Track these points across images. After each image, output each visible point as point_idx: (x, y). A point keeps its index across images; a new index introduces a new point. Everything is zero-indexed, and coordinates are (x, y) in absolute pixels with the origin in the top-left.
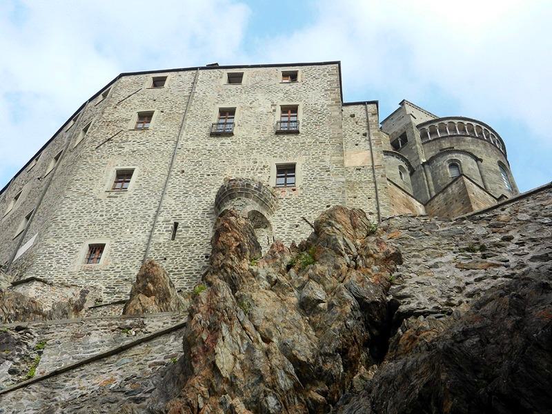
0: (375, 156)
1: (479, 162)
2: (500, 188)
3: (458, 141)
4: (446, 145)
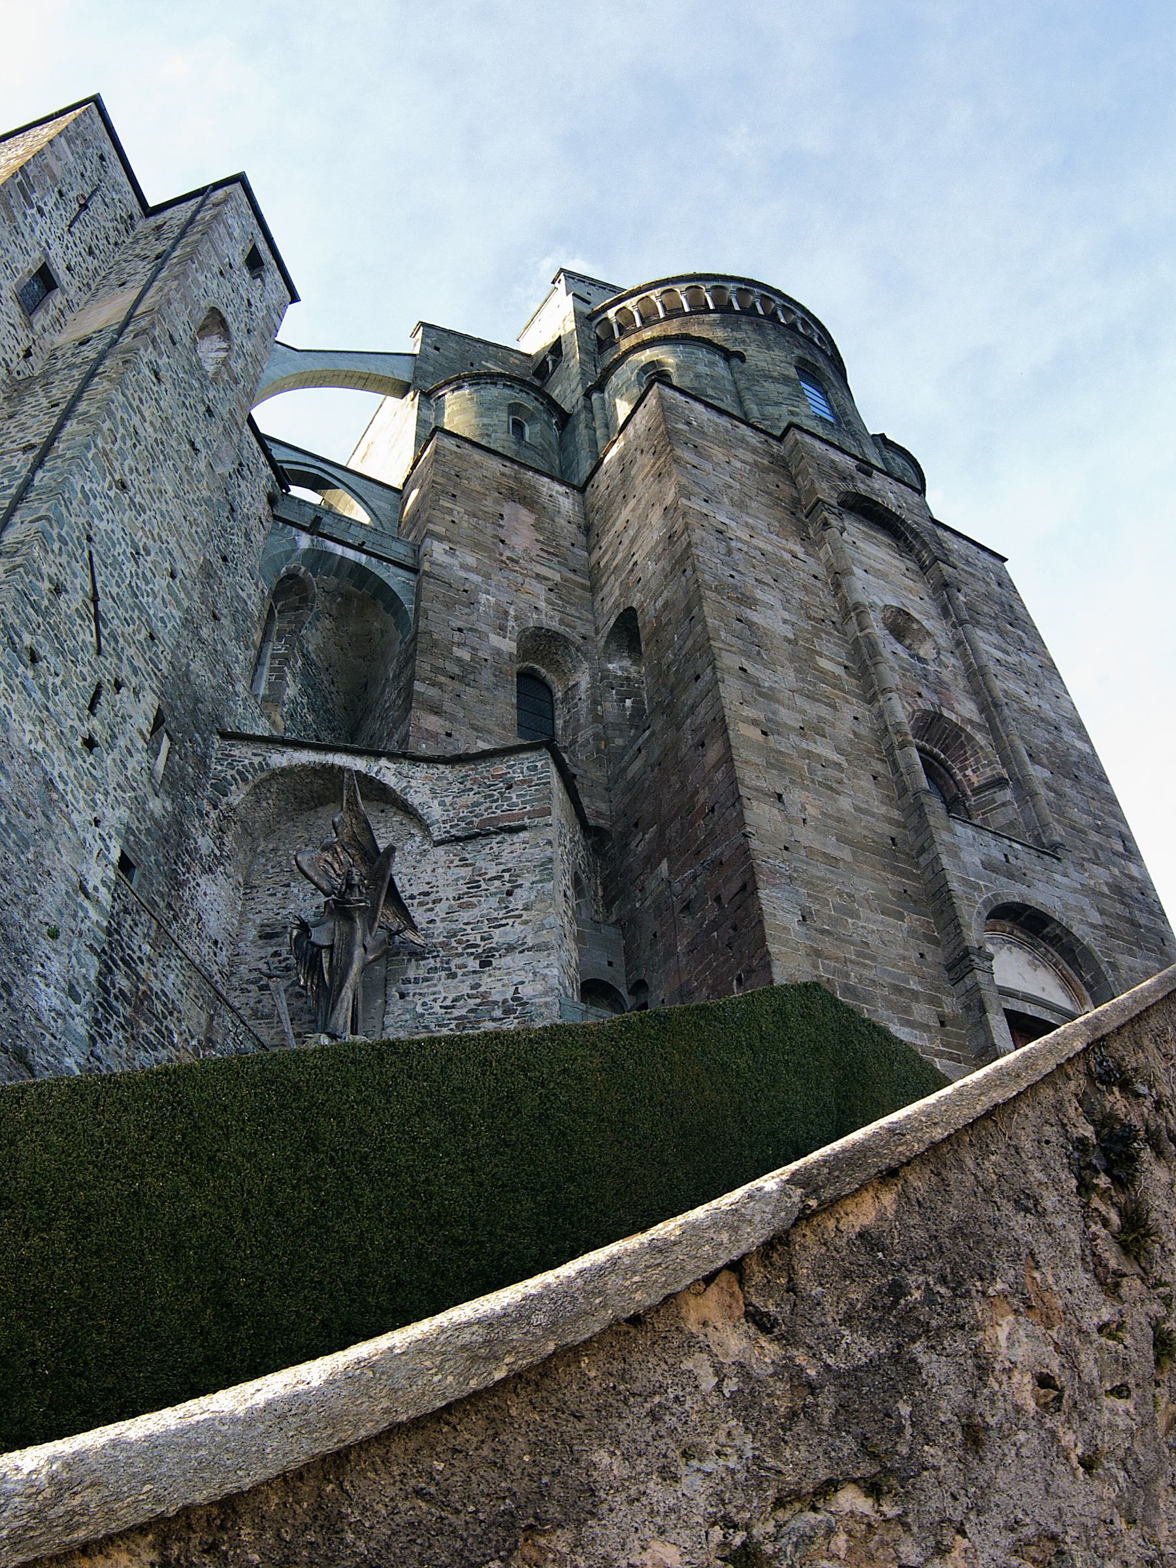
1: (735, 362)
2: (792, 413)
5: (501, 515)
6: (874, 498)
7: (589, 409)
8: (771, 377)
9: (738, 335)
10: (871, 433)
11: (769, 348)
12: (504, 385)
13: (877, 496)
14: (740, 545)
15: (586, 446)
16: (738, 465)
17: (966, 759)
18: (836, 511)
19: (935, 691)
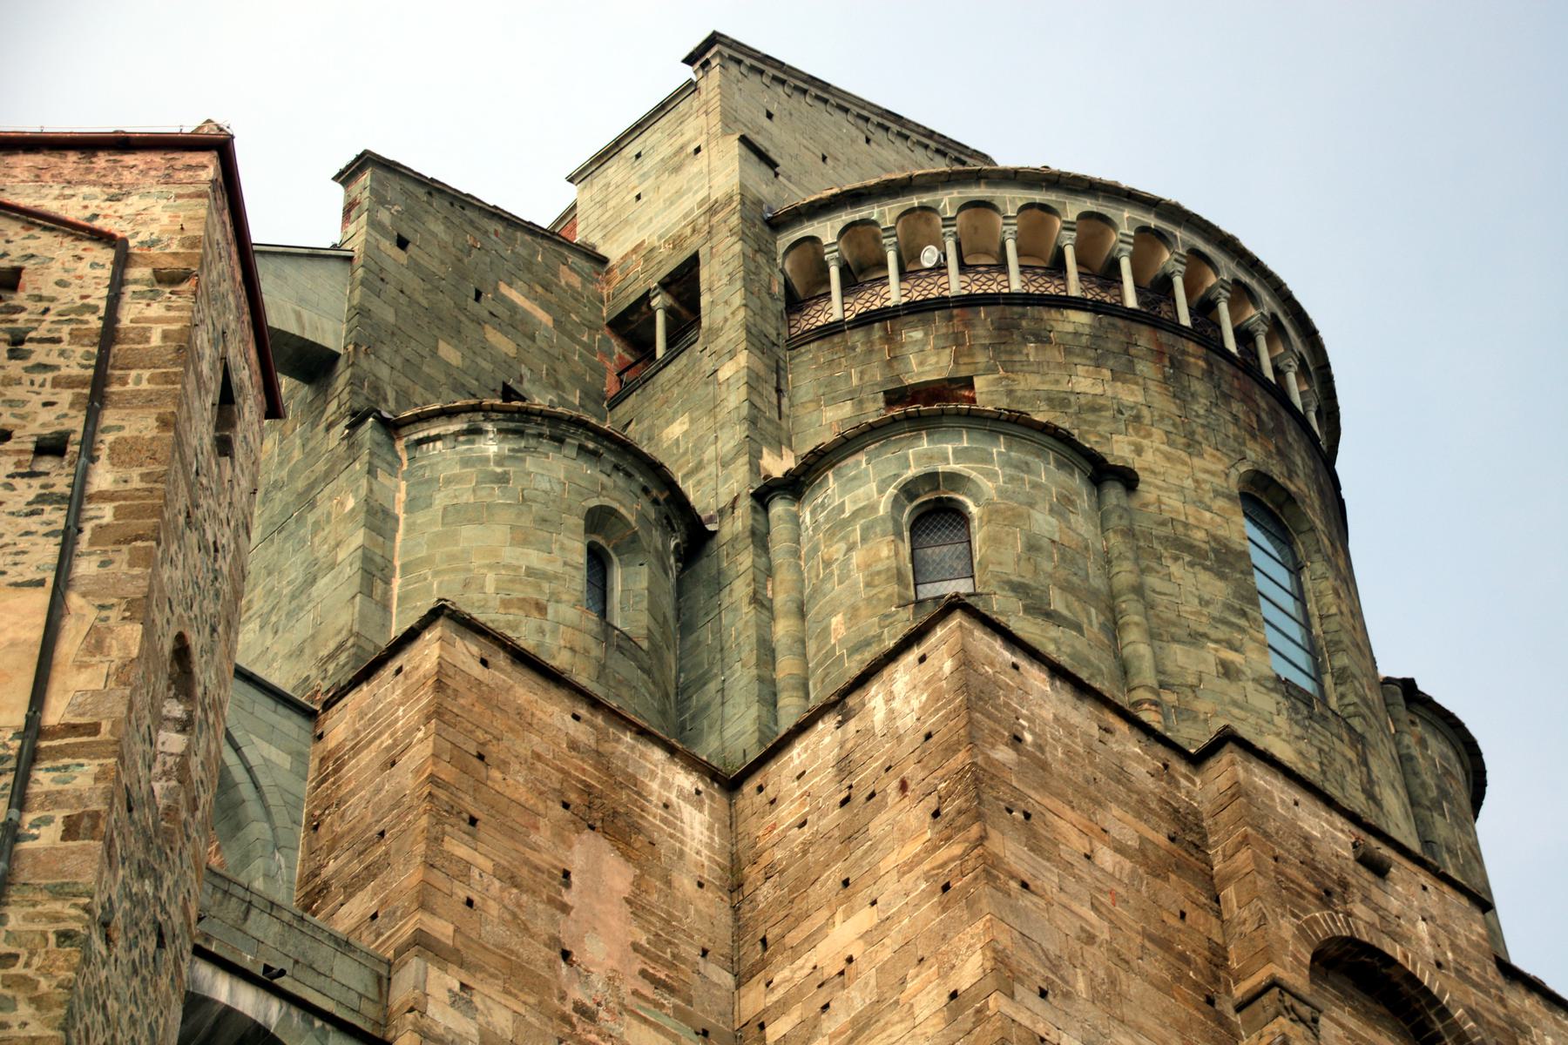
0: (70, 644)
1: (1114, 494)
3: (1005, 335)
4: (925, 359)
5: (566, 874)
7: (760, 538)
8: (1190, 548)
9: (1130, 395)
10: (1384, 671)
11: (1192, 446)
12: (582, 449)
13: (1396, 937)
15: (748, 653)
16: (1106, 858)
18: (1305, 1011)
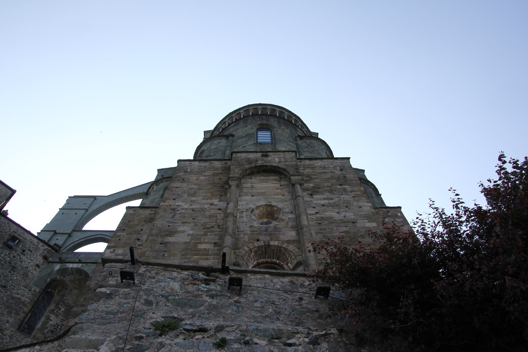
1: (230, 138)
6: (265, 164)
12: (166, 181)
14: (181, 211)
17: (287, 259)
19: (270, 235)
